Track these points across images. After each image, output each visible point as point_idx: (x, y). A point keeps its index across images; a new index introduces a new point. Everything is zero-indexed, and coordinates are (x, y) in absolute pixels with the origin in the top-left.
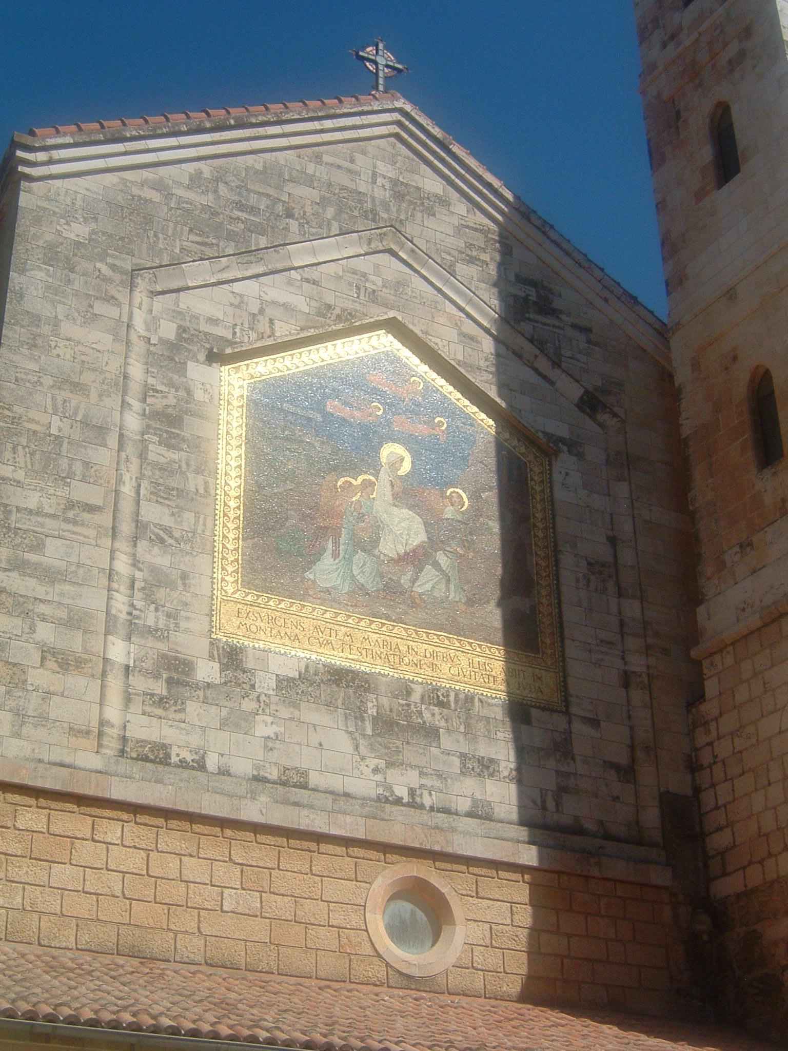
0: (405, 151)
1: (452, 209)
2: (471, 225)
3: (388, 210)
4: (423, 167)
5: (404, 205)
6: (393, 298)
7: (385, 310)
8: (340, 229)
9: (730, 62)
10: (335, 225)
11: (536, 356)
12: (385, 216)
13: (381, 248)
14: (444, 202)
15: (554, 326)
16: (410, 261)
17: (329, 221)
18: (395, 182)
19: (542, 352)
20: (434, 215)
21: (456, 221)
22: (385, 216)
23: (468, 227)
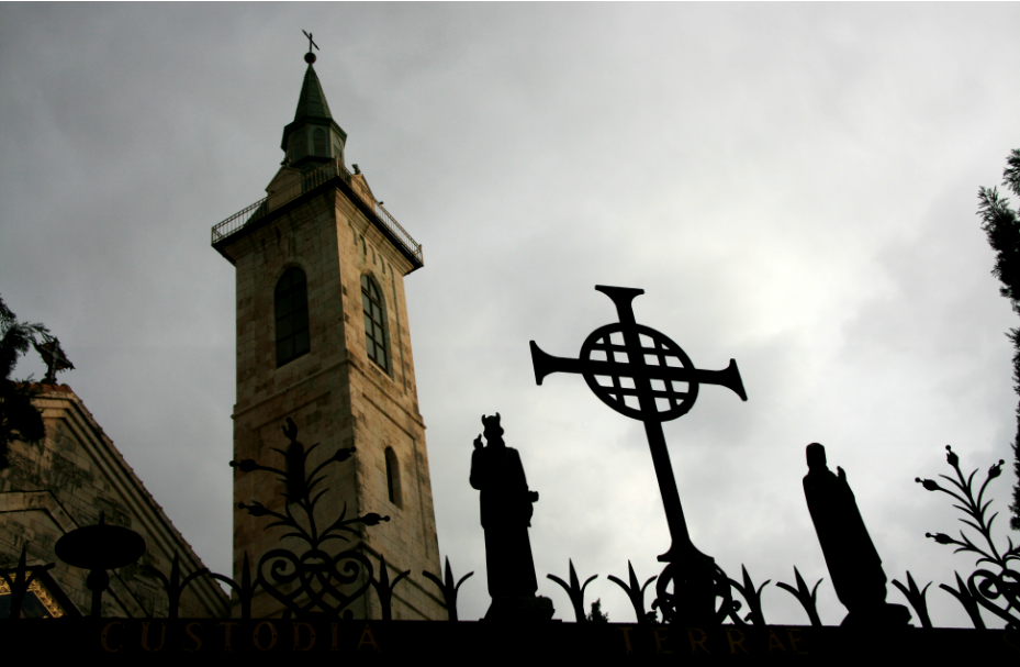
0: (68, 432)
1: (94, 484)
2: (105, 498)
3: (48, 478)
4: (79, 448)
5: (61, 476)
6: (40, 548)
7: (34, 558)
8: (12, 487)
9: (308, 417)
10: (8, 484)
11: (136, 609)
12: (45, 482)
13: (38, 506)
14: (89, 477)
15: (152, 587)
16: (58, 520)
17: (4, 482)
18: (56, 456)
19: (142, 606)
20: (80, 487)
21: (95, 494)
22: (45, 482)
23: (103, 500)
